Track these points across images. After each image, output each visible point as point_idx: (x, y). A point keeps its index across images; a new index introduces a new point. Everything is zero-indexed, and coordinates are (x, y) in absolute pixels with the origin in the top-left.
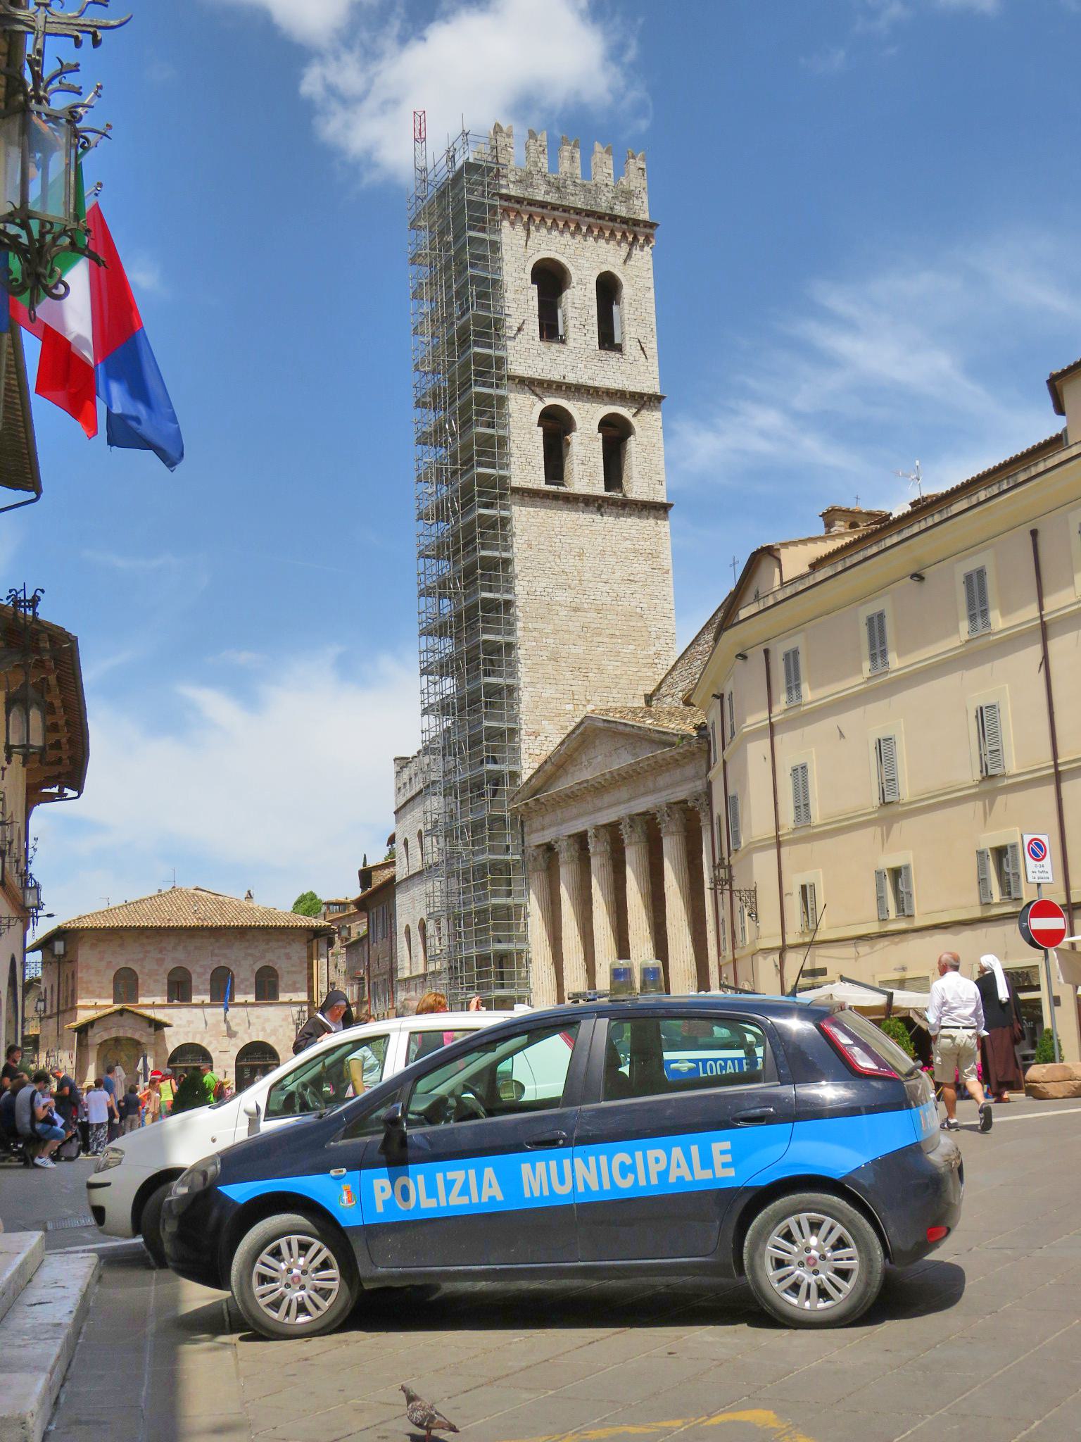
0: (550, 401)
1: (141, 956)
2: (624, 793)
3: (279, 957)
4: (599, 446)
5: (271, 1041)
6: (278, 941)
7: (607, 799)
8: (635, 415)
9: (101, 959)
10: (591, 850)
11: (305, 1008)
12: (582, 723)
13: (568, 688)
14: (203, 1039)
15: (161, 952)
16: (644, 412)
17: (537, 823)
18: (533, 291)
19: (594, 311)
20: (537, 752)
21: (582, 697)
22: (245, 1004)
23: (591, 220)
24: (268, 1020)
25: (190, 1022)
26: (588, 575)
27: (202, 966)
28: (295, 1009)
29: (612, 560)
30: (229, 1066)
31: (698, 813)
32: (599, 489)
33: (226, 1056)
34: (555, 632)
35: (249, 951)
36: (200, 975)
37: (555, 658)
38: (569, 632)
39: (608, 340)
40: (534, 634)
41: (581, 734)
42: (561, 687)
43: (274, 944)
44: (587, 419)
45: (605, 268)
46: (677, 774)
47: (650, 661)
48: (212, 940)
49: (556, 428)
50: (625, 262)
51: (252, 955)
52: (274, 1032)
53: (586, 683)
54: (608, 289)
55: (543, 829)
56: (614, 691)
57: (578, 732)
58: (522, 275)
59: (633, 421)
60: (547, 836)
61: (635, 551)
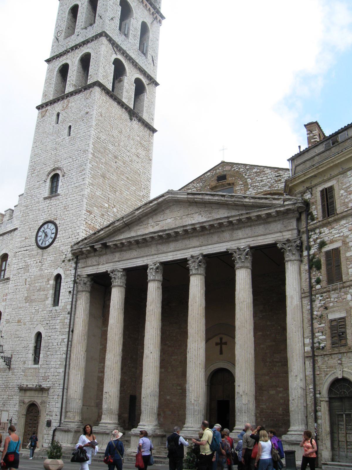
2: (195, 242)
4: (134, 88)
7: (172, 246)
8: (147, 85)
10: (150, 277)
12: (162, 196)
13: (107, 195)
16: (150, 86)
18: (119, 9)
19: (139, 33)
20: (89, 223)
21: (112, 203)
26: (122, 144)
29: (132, 142)
31: (283, 254)
32: (132, 106)
34: (106, 163)
37: (104, 176)
38: (111, 167)
40: (97, 160)
41: (158, 204)
42: (104, 193)
44: (131, 75)
45: (145, 21)
46: (260, 229)
47: (140, 198)
49: (119, 70)
53: (115, 197)
54: (144, 28)
55: (99, 265)
56: (125, 206)
57: (156, 202)
59: (146, 86)
60: (102, 269)
61: (141, 144)
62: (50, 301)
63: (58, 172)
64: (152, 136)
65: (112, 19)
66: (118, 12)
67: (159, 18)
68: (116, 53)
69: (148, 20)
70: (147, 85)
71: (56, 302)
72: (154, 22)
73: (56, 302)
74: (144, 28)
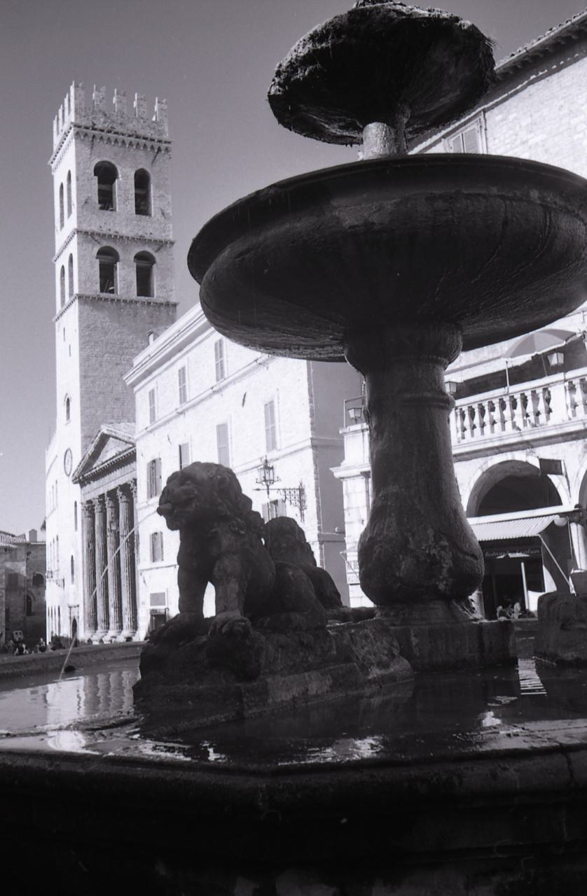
0: (105, 244)
23: (132, 139)
39: (142, 206)
45: (140, 167)
50: (153, 162)
54: (142, 180)
58: (87, 171)
59: (156, 255)
63: (69, 396)
64: (176, 310)
65: (86, 202)
66: (93, 187)
67: (163, 146)
68: (99, 243)
69: (144, 164)
70: (156, 252)
71: (76, 529)
72: (157, 157)
73: (76, 529)
74: (142, 180)
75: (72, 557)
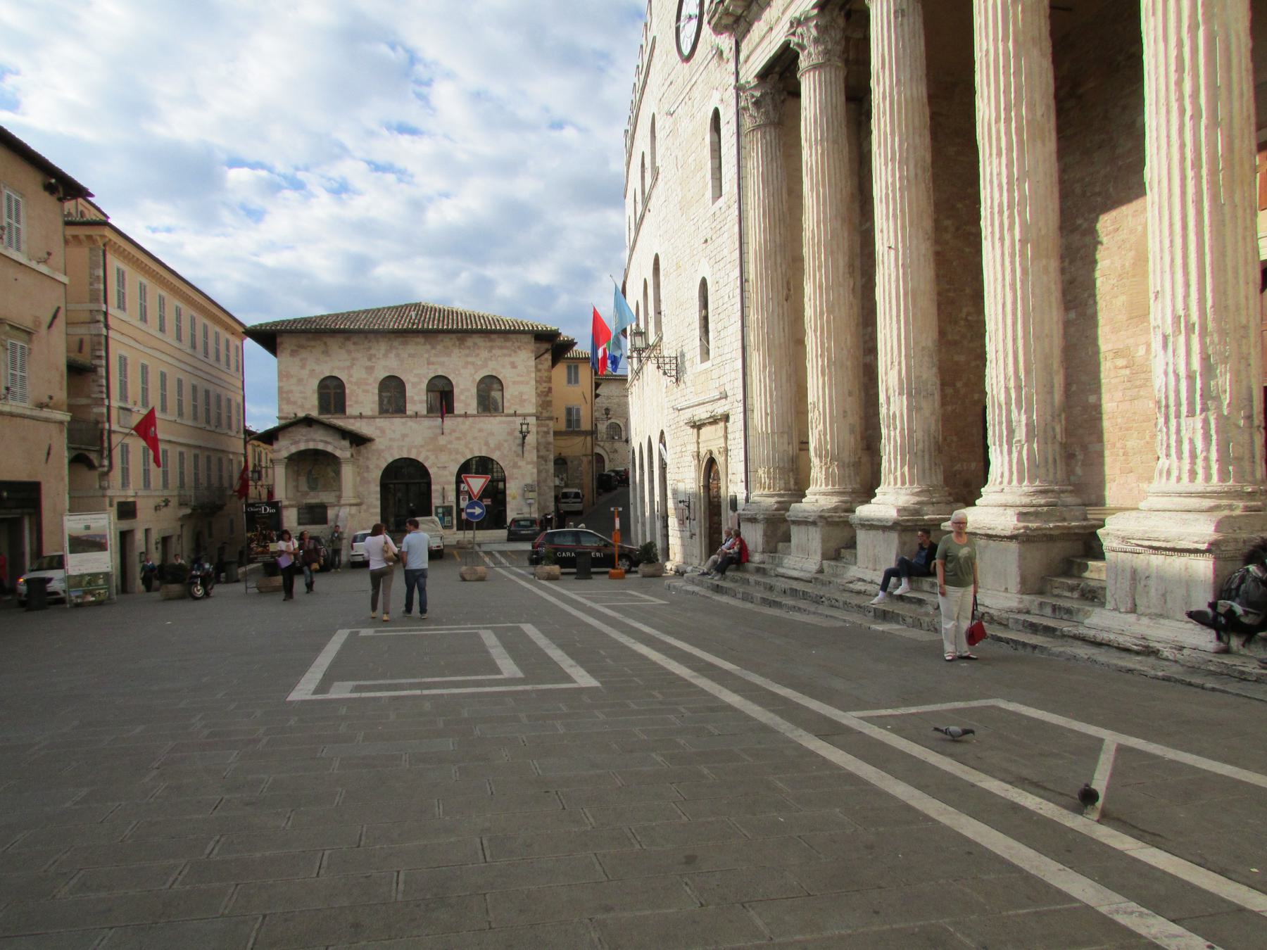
1: (348, 363)
3: (503, 366)
5: (495, 456)
6: (501, 348)
9: (303, 367)
11: (532, 420)
14: (419, 453)
15: (370, 359)
17: (758, 28)
22: (466, 415)
24: (492, 434)
25: (404, 436)
27: (416, 375)
28: (519, 420)
30: (449, 483)
33: (446, 472)
35: (470, 359)
36: (414, 385)
43: (497, 352)
48: (428, 347)
51: (473, 364)
52: (499, 447)
62: (709, 194)
75: (704, 283)
